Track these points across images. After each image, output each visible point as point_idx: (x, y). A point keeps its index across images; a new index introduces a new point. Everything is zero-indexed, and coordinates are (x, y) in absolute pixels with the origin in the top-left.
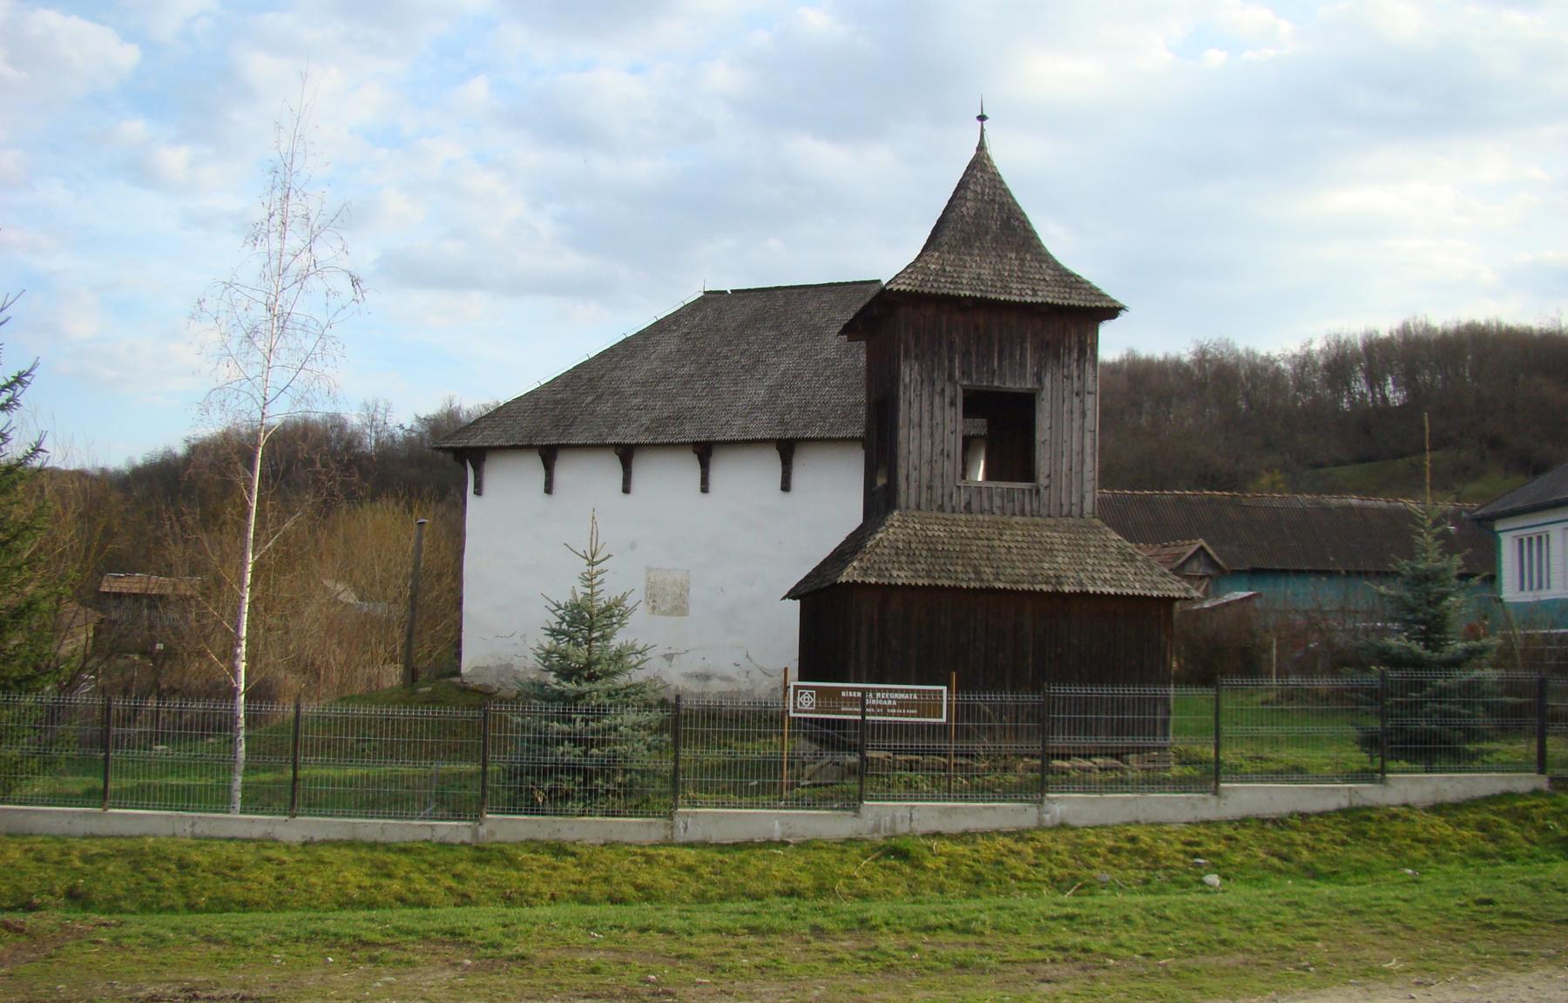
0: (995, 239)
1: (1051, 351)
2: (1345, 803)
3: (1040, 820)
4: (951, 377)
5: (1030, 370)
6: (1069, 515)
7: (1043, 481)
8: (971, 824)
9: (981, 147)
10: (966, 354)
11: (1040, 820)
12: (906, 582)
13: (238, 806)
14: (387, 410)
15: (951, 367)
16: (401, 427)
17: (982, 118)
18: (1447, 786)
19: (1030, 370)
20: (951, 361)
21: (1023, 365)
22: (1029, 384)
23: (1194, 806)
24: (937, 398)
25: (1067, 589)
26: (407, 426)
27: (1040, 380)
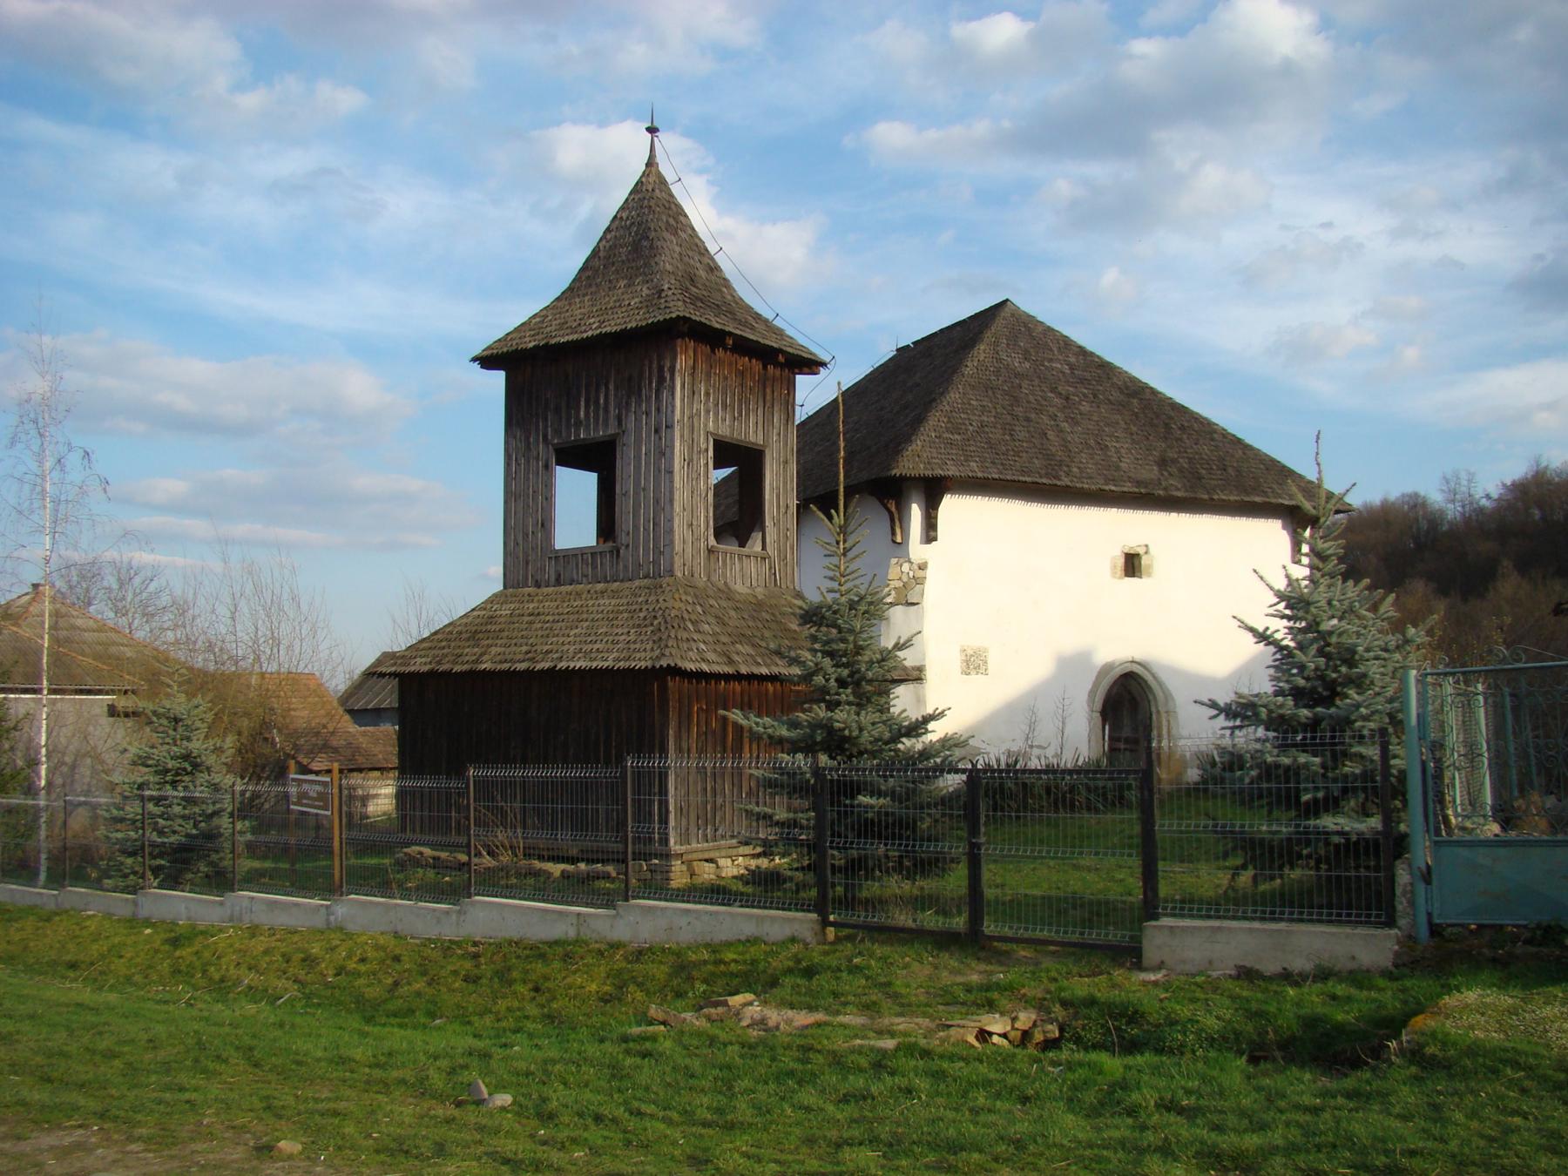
0: (617, 271)
1: (632, 389)
2: (572, 933)
3: (328, 922)
4: (545, 436)
5: (613, 412)
6: (646, 576)
7: (623, 538)
8: (282, 920)
9: (651, 163)
10: (557, 410)
11: (328, 922)
12: (412, 669)
13: (43, 876)
14: (1469, 481)
15: (546, 427)
16: (1488, 497)
17: (652, 130)
18: (683, 921)
19: (613, 412)
20: (546, 419)
21: (606, 410)
22: (611, 431)
23: (439, 921)
24: (533, 462)
25: (539, 667)
26: (1495, 495)
27: (620, 423)
